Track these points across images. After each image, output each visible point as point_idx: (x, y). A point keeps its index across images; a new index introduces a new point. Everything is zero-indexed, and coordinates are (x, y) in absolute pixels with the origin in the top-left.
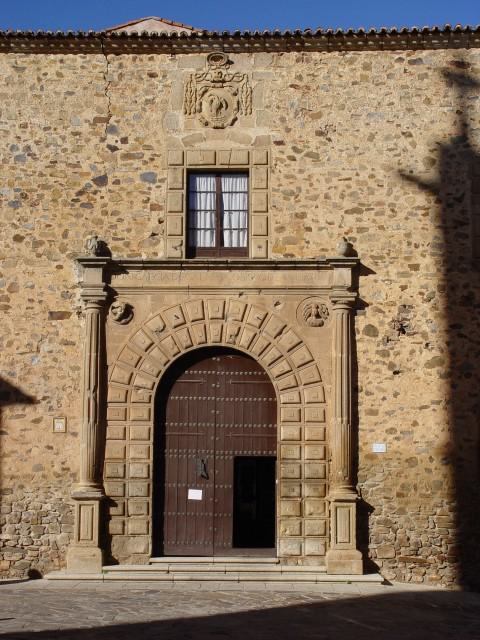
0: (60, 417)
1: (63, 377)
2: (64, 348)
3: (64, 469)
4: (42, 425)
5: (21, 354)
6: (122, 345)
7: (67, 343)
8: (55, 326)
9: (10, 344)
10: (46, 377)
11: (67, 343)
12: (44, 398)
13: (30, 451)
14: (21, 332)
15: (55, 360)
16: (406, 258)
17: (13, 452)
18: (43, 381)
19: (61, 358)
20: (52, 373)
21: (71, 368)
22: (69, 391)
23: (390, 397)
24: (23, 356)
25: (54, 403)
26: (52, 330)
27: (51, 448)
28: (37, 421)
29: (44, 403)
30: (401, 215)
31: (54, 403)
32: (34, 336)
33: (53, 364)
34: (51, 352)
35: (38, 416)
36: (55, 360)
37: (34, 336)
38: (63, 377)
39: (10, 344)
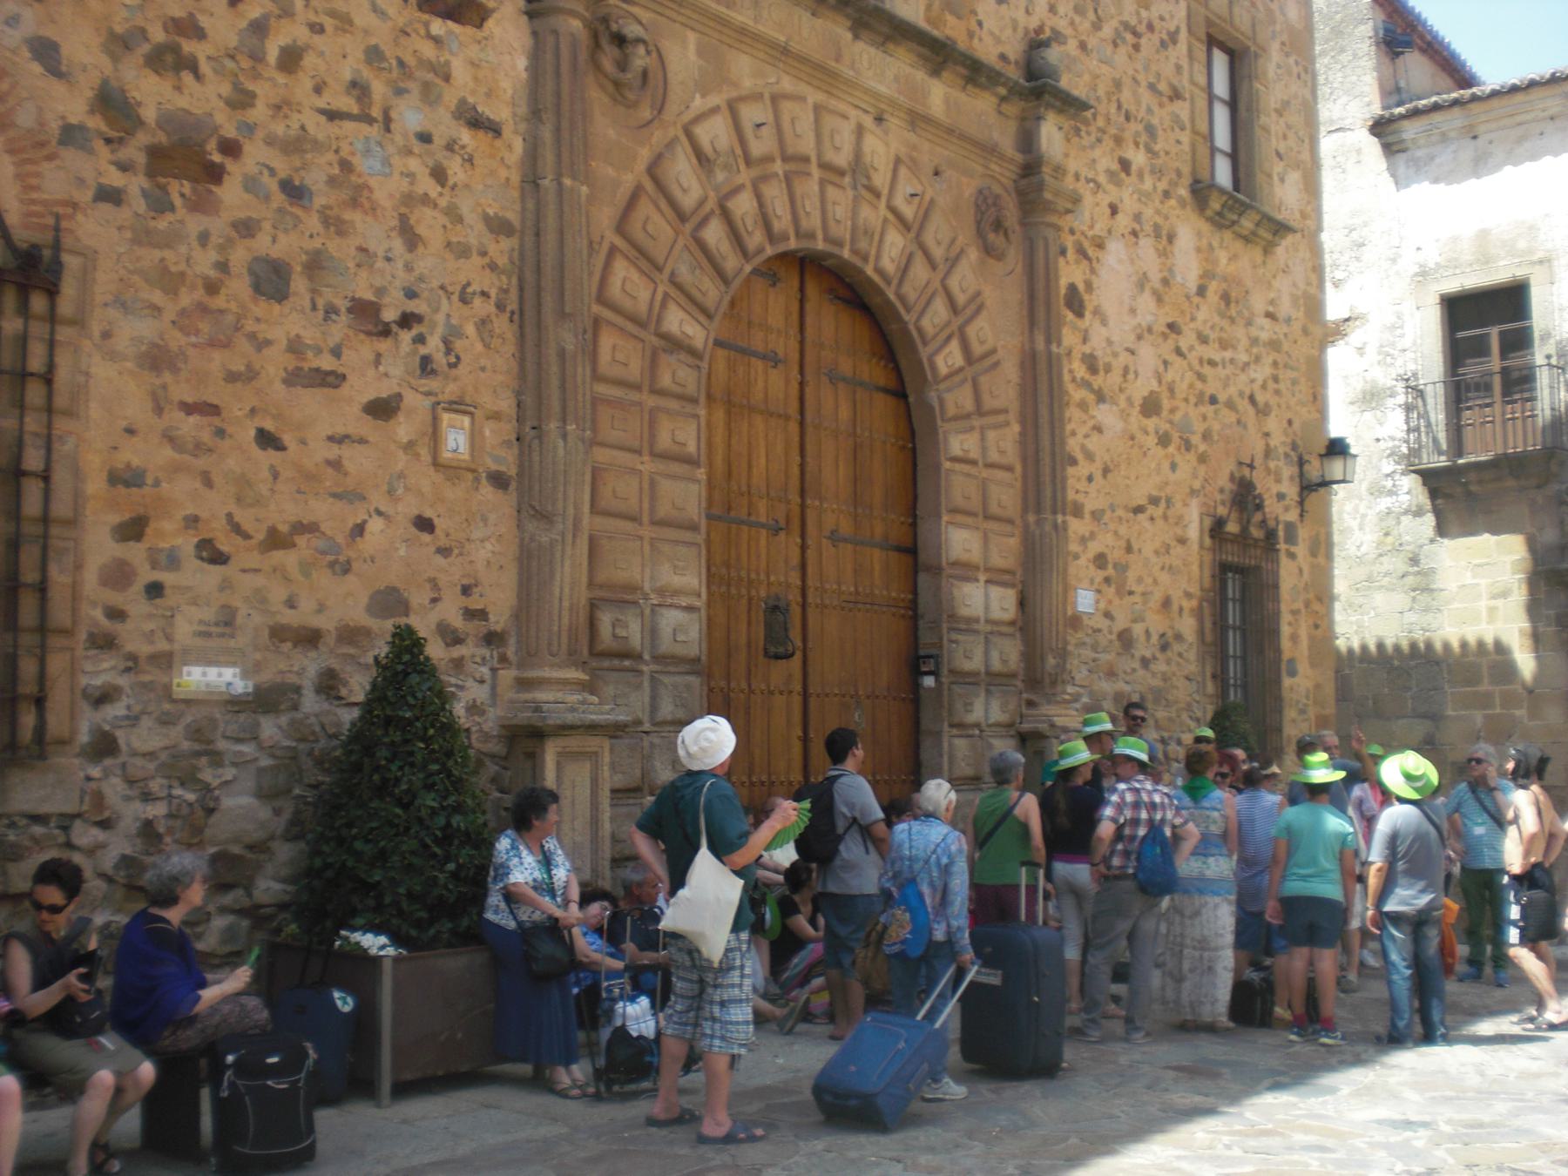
0: (458, 406)
1: (463, 252)
2: (466, 136)
3: (470, 614)
4: (404, 428)
5: (332, 115)
6: (629, 180)
7: (477, 122)
8: (437, 40)
9: (291, 59)
10: (412, 240)
11: (477, 122)
12: (407, 320)
13: (359, 530)
14: (328, 23)
15: (439, 174)
16: (1118, 140)
17: (301, 528)
18: (398, 245)
19: (456, 170)
20: (428, 223)
21: (487, 219)
22: (480, 307)
23: (1098, 475)
24: (335, 129)
25: (434, 345)
26: (428, 50)
27: (424, 524)
28: (382, 409)
29: (406, 337)
30: (1107, 31)
31: (434, 345)
32: (374, 55)
33: (433, 189)
34: (425, 138)
35: (384, 390)
36: (439, 174)
37: (374, 55)
38: (463, 252)
39: (291, 59)
